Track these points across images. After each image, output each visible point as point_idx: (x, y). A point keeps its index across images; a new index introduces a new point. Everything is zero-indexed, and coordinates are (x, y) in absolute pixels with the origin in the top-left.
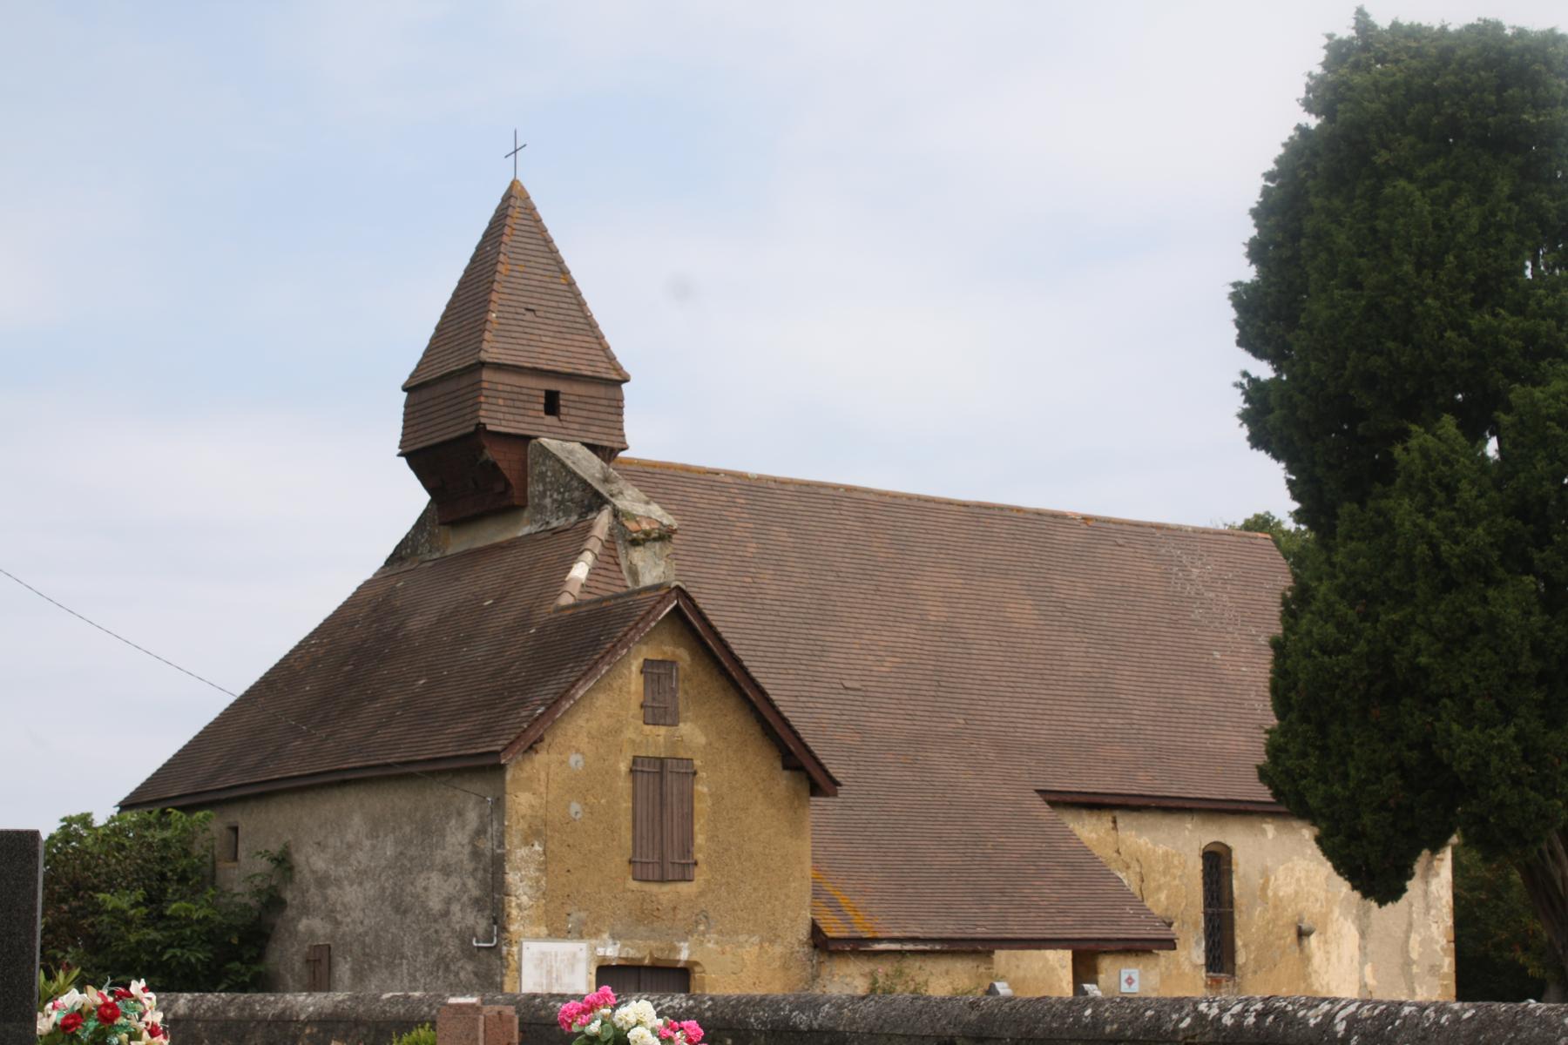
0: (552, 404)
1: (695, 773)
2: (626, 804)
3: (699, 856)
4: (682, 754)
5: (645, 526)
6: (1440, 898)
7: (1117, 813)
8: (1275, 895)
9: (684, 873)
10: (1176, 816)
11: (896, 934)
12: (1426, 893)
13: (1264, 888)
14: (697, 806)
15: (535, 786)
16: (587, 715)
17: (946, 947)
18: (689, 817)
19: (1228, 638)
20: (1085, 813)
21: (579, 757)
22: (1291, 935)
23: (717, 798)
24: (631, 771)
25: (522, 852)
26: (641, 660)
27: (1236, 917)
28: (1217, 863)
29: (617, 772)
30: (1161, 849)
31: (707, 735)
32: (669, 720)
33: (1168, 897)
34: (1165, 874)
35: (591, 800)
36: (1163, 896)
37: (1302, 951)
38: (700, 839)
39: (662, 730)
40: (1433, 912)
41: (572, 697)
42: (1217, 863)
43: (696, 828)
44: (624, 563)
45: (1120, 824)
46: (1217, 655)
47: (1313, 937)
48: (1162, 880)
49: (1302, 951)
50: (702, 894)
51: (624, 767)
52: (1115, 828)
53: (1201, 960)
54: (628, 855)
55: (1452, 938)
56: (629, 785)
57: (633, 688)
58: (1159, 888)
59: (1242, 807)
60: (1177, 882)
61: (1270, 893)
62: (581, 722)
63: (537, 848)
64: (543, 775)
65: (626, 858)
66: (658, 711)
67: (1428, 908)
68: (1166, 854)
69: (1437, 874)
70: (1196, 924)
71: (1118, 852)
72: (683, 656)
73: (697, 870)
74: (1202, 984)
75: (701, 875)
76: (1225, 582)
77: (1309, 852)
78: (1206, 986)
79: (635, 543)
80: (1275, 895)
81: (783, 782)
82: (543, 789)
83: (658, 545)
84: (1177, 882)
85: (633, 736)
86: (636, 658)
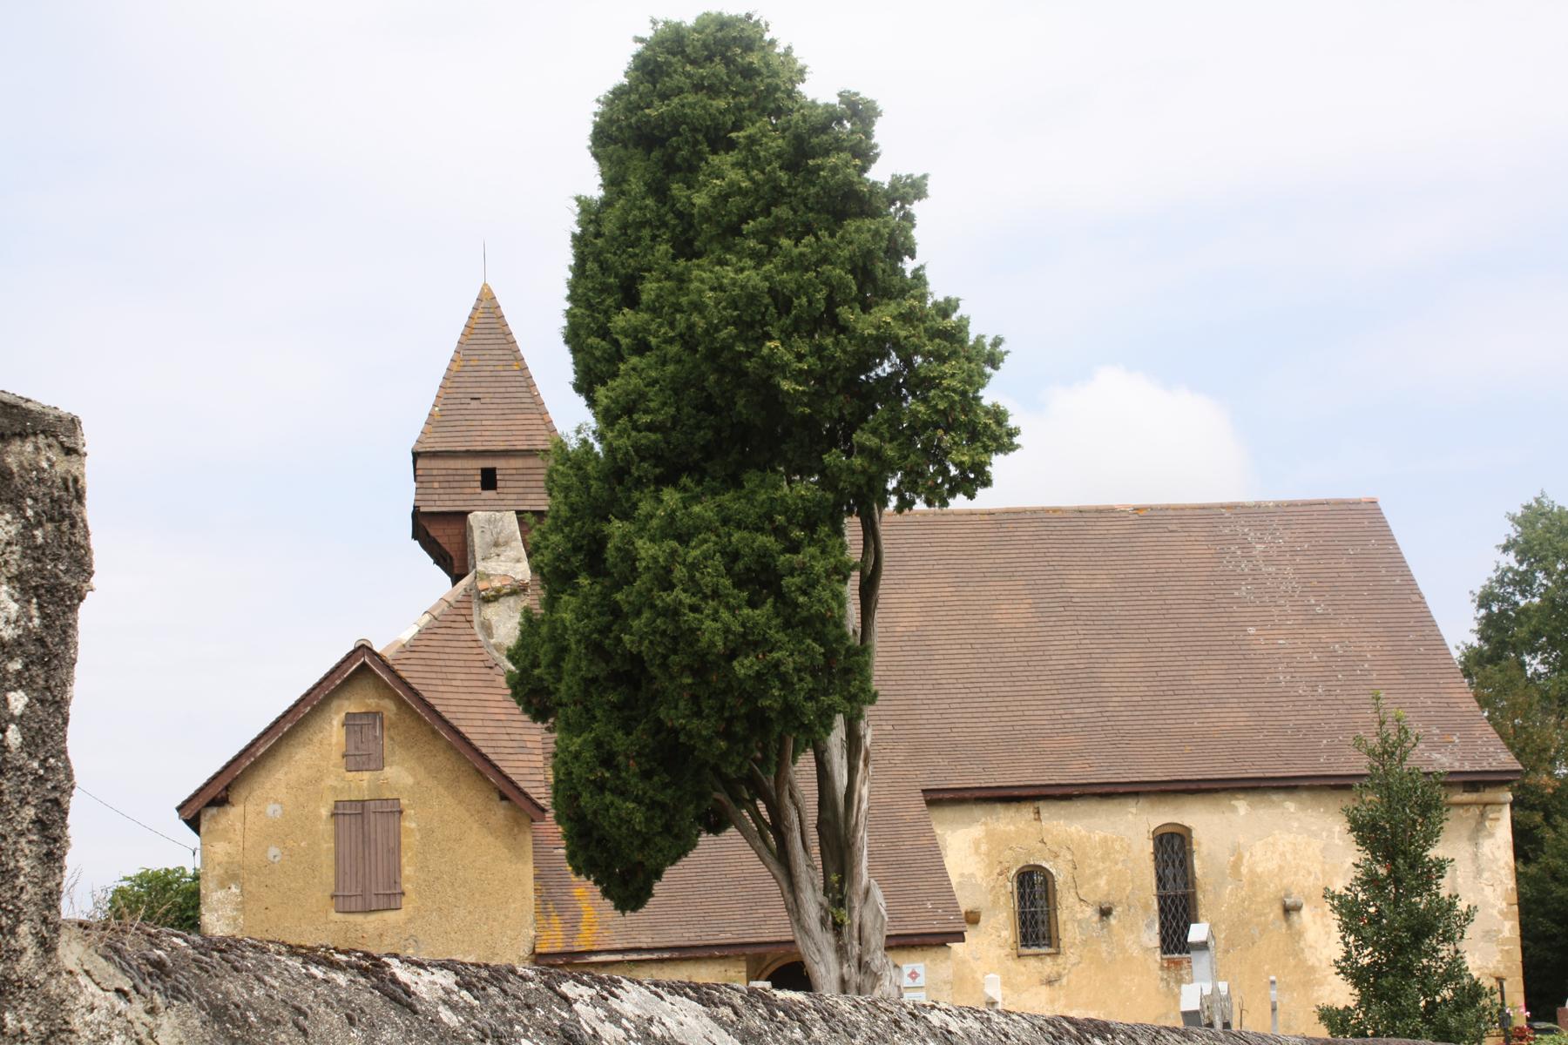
0: (489, 480)
1: (401, 812)
2: (328, 845)
3: (407, 887)
4: (388, 795)
5: (496, 584)
6: (1495, 860)
7: (1041, 804)
8: (1252, 871)
9: (391, 898)
10: (1116, 801)
11: (618, 946)
12: (1475, 857)
13: (1236, 866)
14: (404, 840)
15: (231, 835)
16: (285, 769)
17: (676, 955)
18: (395, 851)
19: (1275, 611)
20: (999, 808)
21: (277, 807)
22: (1277, 910)
23: (427, 833)
24: (333, 815)
25: (220, 894)
26: (343, 714)
27: (1200, 896)
28: (1173, 849)
29: (319, 817)
30: (1097, 836)
31: (414, 776)
32: (373, 766)
33: (1109, 883)
34: (1103, 859)
35: (290, 843)
36: (1102, 882)
37: (1290, 926)
38: (408, 871)
39: (366, 775)
40: (1486, 875)
41: (253, 755)
42: (1173, 849)
43: (404, 860)
44: (476, 619)
45: (1044, 814)
46: (1252, 630)
47: (1305, 911)
48: (1101, 866)
49: (1290, 926)
50: (410, 921)
51: (325, 812)
52: (1039, 819)
53: (1155, 941)
54: (331, 890)
55: (1514, 899)
56: (331, 827)
57: (334, 740)
58: (1097, 874)
59: (1193, 786)
60: (1120, 866)
61: (1244, 870)
62: (278, 776)
63: (234, 889)
64: (239, 826)
65: (328, 894)
66: (357, 759)
67: (1479, 872)
68: (1105, 840)
69: (1491, 835)
70: (1146, 907)
71: (1042, 841)
72: (389, 707)
73: (404, 899)
74: (1157, 966)
75: (409, 905)
76: (1294, 553)
77: (1337, 829)
78: (1162, 968)
79: (487, 600)
80: (1252, 871)
81: (500, 812)
82: (239, 838)
83: (512, 600)
84: (1120, 866)
85: (335, 783)
86: (337, 713)
